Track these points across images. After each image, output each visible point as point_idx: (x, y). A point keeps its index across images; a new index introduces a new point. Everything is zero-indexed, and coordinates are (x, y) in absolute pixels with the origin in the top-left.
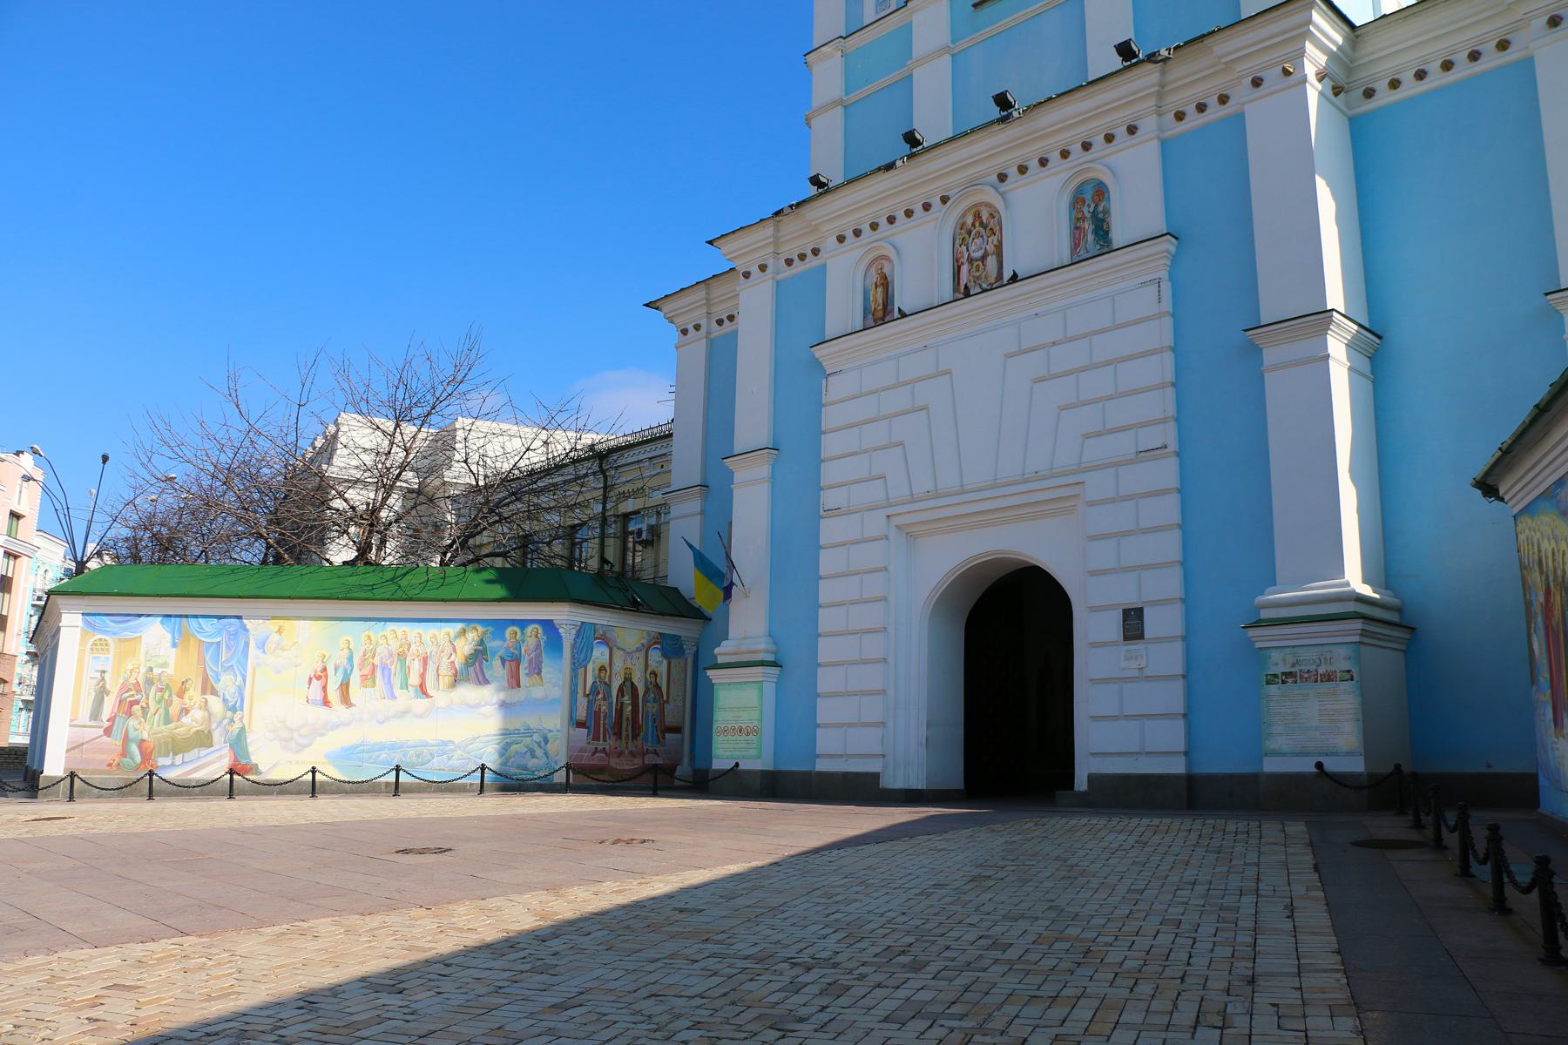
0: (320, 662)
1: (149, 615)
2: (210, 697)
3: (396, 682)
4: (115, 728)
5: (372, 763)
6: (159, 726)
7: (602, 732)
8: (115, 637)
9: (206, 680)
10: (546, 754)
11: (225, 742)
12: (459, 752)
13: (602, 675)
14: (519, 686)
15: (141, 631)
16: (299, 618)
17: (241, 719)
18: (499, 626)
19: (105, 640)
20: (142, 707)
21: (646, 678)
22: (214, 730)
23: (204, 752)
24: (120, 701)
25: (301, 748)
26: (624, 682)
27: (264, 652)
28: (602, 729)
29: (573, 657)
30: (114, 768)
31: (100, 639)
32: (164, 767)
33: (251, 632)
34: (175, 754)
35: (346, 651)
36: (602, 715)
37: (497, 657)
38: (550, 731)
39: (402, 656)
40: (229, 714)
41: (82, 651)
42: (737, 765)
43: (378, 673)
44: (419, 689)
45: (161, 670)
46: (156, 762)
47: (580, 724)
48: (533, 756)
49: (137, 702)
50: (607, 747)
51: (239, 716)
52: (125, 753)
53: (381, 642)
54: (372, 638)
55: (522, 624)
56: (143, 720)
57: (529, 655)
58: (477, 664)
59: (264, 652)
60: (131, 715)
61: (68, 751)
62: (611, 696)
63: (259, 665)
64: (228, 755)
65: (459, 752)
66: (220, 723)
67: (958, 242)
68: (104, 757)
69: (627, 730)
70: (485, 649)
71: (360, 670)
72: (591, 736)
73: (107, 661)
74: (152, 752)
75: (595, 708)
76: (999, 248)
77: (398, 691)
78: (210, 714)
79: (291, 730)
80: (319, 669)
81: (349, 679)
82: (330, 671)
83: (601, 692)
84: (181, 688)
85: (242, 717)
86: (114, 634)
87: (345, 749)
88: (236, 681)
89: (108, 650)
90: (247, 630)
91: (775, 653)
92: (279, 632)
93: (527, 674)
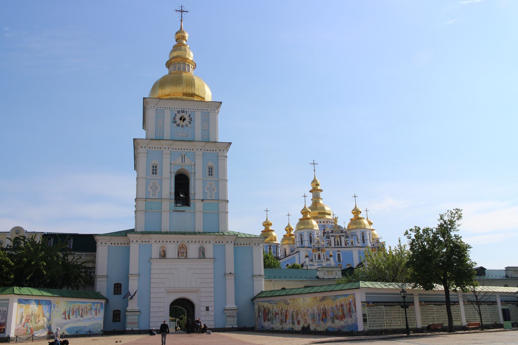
2: (44, 318)
3: (78, 314)
9: (43, 314)
10: (101, 328)
18: (94, 303)
32: (35, 333)
33: (52, 304)
34: (37, 330)
35: (69, 308)
39: (79, 309)
41: (18, 308)
42: (132, 329)
43: (75, 312)
49: (30, 319)
52: (27, 331)
55: (97, 303)
61: (15, 331)
63: (53, 311)
67: (179, 249)
68: (23, 332)
76: (186, 252)
77: (78, 316)
90: (51, 303)
91: (139, 310)
92: (57, 304)
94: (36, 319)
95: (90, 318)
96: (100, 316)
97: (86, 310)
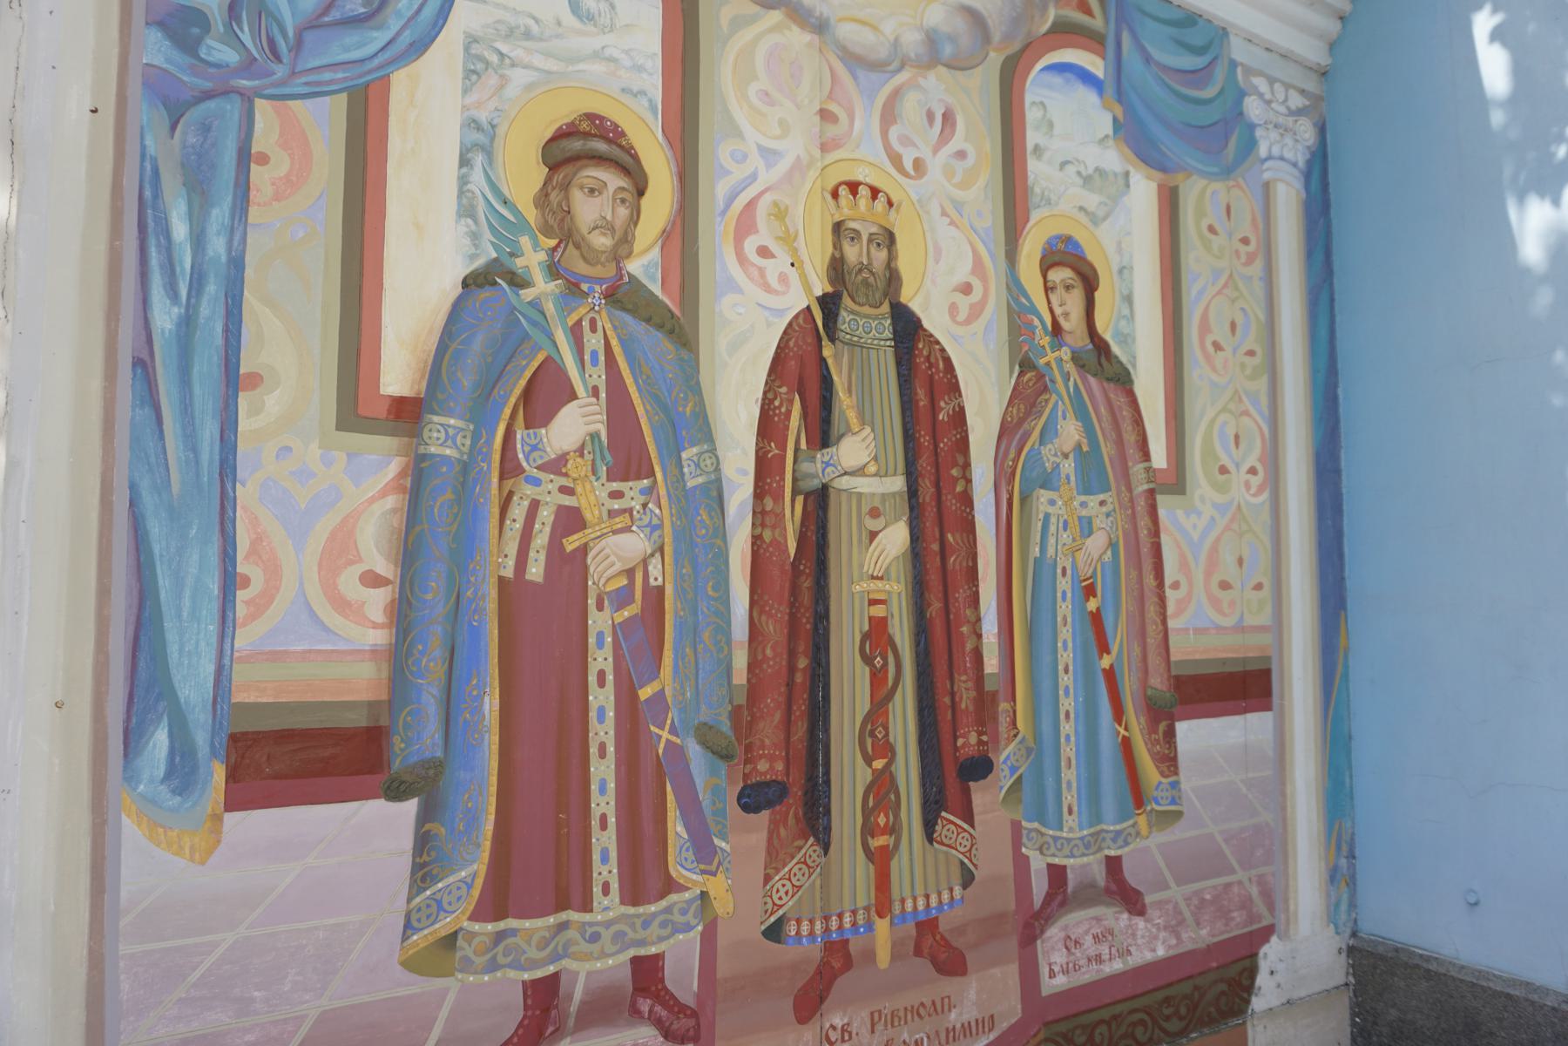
7: (604, 803)
21: (1014, 286)
26: (829, 304)
28: (603, 771)
36: (600, 622)
62: (704, 431)
83: (585, 377)
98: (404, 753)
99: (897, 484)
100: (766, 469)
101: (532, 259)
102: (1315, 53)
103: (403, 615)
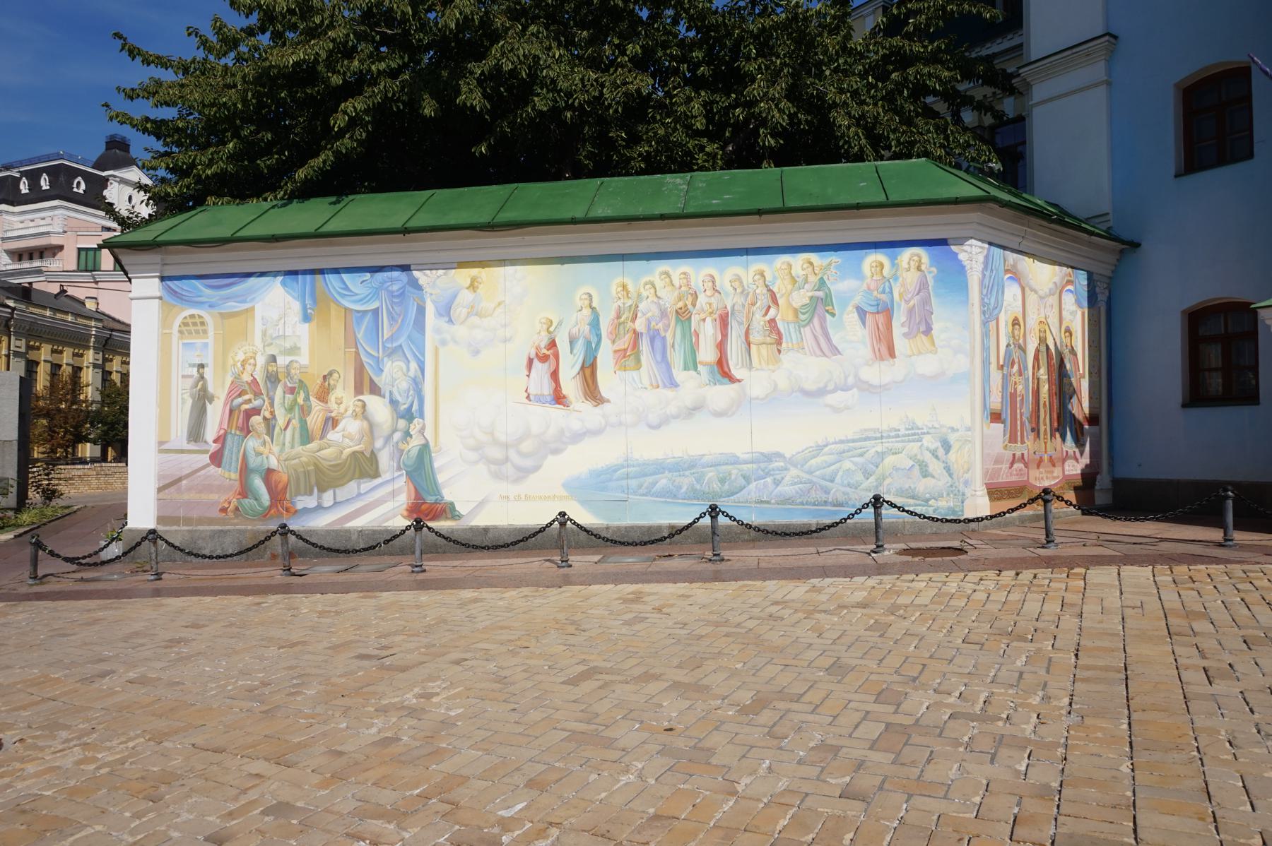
0: (544, 333)
1: (262, 274)
2: (370, 399)
3: (677, 358)
4: (226, 452)
5: (643, 495)
6: (293, 447)
7: (1019, 428)
8: (215, 311)
9: (360, 370)
11: (399, 469)
12: (794, 472)
13: (1016, 332)
14: (892, 354)
15: (254, 299)
16: (503, 262)
17: (422, 431)
19: (200, 317)
20: (265, 418)
22: (380, 450)
23: (366, 485)
24: (231, 411)
25: (524, 473)
27: (450, 321)
28: (1019, 422)
29: (983, 304)
30: (231, 515)
31: (192, 316)
32: (306, 511)
33: (427, 289)
34: (322, 490)
35: (587, 312)
36: (1018, 399)
37: (850, 308)
38: (953, 430)
39: (683, 315)
40: (402, 423)
43: (645, 346)
44: (716, 367)
45: (288, 359)
46: (293, 503)
47: (996, 417)
48: (925, 474)
49: (257, 411)
50: (1026, 453)
51: (418, 427)
53: (645, 294)
54: (631, 287)
56: (267, 438)
57: (907, 302)
58: (816, 321)
59: (450, 321)
60: (249, 432)
61: (160, 490)
62: (1027, 370)
63: (444, 343)
64: (406, 488)
65: (794, 472)
66: (388, 439)
68: (214, 497)
69: (1045, 425)
70: (829, 296)
71: (614, 342)
72: (1008, 436)
73: (206, 348)
74: (285, 488)
75: (1010, 389)
77: (679, 374)
78: (371, 426)
79: (506, 446)
80: (543, 344)
81: (595, 358)
82: (563, 346)
83: (1016, 360)
84: (322, 386)
85: (423, 428)
86: (211, 306)
87: (596, 474)
88: (408, 370)
89: (205, 332)
90: (420, 288)
92: (473, 286)
93: (906, 335)
94: (302, 408)
95: (810, 386)
96: (927, 365)
97: (759, 321)
98: (1003, 416)
99: (1046, 377)
100: (1033, 374)
101: (1011, 343)
102: (1108, 273)
103: (1002, 398)
